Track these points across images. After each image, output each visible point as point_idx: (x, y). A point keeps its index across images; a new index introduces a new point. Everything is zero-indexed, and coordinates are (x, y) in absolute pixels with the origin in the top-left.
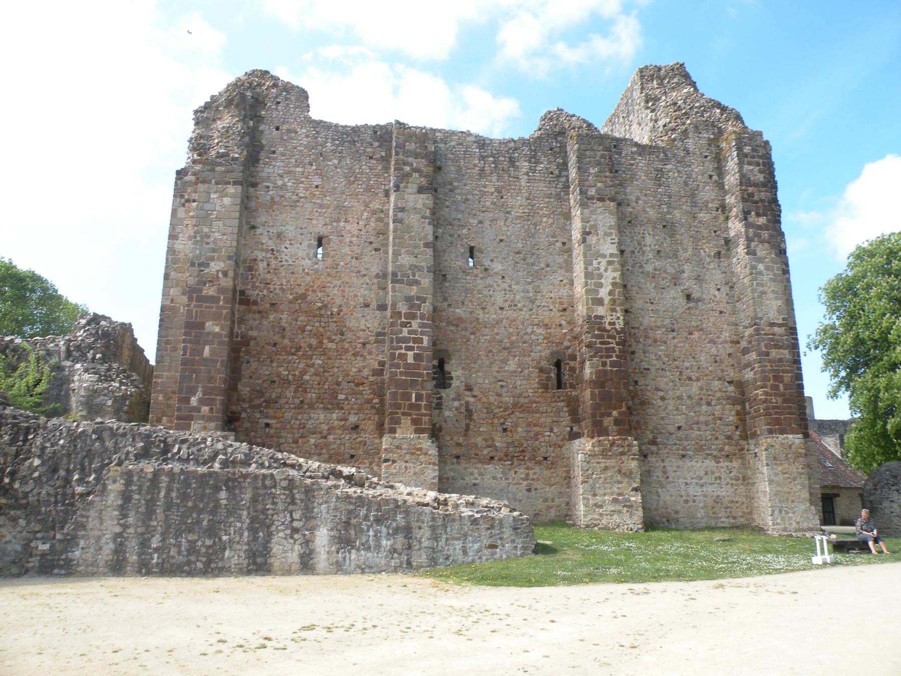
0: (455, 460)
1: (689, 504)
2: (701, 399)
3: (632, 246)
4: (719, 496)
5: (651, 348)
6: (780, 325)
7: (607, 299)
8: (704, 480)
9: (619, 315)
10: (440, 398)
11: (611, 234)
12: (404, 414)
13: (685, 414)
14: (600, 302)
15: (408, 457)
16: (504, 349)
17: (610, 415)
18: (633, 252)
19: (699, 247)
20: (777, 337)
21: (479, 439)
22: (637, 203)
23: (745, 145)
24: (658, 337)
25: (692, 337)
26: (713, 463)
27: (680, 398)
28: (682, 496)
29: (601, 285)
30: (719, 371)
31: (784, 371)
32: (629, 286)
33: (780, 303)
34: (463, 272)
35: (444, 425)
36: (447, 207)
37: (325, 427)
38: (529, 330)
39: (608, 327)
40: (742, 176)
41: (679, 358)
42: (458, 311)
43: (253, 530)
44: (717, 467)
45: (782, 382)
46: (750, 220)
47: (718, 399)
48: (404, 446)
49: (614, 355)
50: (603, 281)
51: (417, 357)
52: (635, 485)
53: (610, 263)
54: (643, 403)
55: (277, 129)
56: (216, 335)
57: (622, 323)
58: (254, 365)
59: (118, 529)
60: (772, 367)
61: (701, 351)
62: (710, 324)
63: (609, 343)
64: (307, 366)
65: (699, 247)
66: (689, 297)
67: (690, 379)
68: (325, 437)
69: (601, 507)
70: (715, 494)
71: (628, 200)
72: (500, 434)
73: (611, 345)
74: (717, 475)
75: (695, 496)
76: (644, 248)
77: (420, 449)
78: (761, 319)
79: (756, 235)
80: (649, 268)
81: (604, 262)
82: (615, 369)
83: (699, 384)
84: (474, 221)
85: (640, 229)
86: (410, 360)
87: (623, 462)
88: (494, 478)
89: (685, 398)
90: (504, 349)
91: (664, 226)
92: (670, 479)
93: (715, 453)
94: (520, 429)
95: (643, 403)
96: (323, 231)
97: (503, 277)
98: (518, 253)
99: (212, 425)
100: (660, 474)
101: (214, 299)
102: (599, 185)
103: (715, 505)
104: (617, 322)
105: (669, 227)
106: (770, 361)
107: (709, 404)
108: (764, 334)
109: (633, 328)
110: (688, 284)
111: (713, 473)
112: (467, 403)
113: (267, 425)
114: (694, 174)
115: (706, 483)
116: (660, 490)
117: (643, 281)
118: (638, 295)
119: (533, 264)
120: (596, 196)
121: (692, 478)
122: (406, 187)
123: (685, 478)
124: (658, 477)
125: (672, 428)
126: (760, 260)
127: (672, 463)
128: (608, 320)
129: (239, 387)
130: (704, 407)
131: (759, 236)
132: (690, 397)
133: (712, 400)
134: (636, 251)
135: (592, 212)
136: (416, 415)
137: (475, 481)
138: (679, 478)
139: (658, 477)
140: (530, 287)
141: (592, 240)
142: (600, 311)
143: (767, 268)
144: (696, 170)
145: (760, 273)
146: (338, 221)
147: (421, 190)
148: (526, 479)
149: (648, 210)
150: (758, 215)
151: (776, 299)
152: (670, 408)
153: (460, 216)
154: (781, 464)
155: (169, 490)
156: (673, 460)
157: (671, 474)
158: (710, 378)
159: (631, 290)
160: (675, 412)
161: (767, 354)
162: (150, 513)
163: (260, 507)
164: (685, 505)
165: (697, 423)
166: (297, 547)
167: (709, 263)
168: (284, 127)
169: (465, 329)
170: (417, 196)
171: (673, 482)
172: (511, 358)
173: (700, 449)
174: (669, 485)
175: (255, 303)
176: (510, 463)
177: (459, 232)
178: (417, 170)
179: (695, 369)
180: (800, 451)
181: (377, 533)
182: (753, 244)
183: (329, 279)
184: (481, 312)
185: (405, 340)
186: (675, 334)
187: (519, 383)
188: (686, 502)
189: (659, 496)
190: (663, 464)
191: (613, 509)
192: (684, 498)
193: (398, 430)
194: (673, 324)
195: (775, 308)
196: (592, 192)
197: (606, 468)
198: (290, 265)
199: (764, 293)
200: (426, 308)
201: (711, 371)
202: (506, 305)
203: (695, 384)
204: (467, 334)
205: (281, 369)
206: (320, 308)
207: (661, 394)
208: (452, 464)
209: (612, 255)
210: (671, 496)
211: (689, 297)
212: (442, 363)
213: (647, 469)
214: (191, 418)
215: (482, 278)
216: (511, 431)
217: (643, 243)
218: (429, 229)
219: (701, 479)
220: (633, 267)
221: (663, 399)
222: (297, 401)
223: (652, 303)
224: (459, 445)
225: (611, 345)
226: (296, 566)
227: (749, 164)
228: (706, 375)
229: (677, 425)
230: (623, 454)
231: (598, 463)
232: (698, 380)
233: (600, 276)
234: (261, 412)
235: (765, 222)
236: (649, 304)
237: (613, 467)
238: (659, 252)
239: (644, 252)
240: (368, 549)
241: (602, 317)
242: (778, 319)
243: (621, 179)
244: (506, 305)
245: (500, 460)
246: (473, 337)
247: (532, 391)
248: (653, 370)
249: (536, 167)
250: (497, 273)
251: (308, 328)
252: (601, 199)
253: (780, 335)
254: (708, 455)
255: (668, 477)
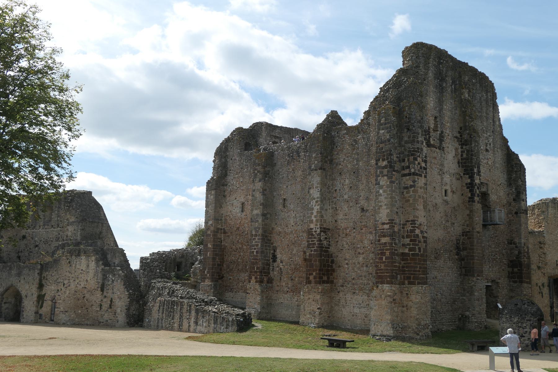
0: (276, 292)
1: (354, 317)
2: (364, 264)
3: (340, 186)
4: (366, 314)
5: (344, 238)
6: (387, 224)
7: (314, 219)
8: (362, 305)
9: (318, 227)
10: (273, 267)
11: (318, 187)
12: (253, 275)
13: (356, 271)
14: (311, 222)
15: (253, 292)
16: (293, 244)
17: (312, 274)
18: (340, 190)
19: (369, 181)
20: (385, 230)
21: (284, 284)
22: (344, 162)
23: (382, 118)
24: (347, 232)
25: (362, 231)
26: (366, 297)
27: (354, 263)
28: (351, 313)
29: (312, 213)
30: (373, 249)
31: (387, 250)
32: (337, 208)
33: (388, 211)
34: (282, 211)
35: (274, 278)
36: (277, 182)
37: (243, 279)
38: (301, 234)
39: (314, 233)
40: (378, 138)
41: (356, 243)
42: (279, 228)
43: (180, 319)
44: (368, 299)
45: (385, 255)
46: (379, 164)
47: (371, 264)
48: (252, 288)
49: (315, 246)
50: (313, 211)
51: (257, 252)
52: (319, 307)
53: (317, 202)
54: (339, 266)
55: (231, 159)
56: (210, 248)
57: (319, 231)
58: (227, 256)
59: (158, 317)
60: (380, 247)
61: (366, 238)
62: (371, 223)
63: (314, 241)
64: (239, 256)
65: (369, 181)
66: (363, 210)
67: (359, 253)
68: (243, 283)
69: (305, 315)
70: (365, 313)
71: (340, 161)
72: (290, 281)
73: (315, 242)
74: (367, 303)
75: (357, 313)
76: (345, 187)
77: (256, 289)
78: (378, 221)
79: (381, 172)
80: (346, 197)
81: (314, 201)
82: (315, 253)
83: (363, 256)
84: (285, 187)
85: (343, 176)
86: (255, 254)
87: (315, 296)
88: (288, 300)
89: (357, 263)
90: (293, 244)
91: (354, 172)
92: (348, 304)
93: (367, 292)
94: (296, 279)
95: (339, 266)
96: (243, 200)
97: (294, 211)
98: (299, 199)
99: (210, 281)
100: (344, 301)
101: (210, 235)
102: (316, 162)
103: (365, 318)
104: (317, 230)
105: (356, 172)
106: (380, 244)
107: (367, 266)
108: (379, 230)
109: (338, 229)
110: (363, 202)
111: (366, 302)
112: (281, 269)
113: (230, 278)
114: (371, 137)
115: (362, 307)
116: (343, 309)
117: (343, 204)
118: (341, 212)
119: (303, 203)
120: (315, 168)
121: (357, 304)
122: (255, 180)
123: (354, 304)
124: (343, 302)
125: (350, 279)
126: (381, 187)
127: (349, 296)
128: (314, 230)
129: (224, 265)
130: (365, 268)
131: (381, 172)
132: (359, 263)
133: (368, 264)
134: (341, 189)
135: (312, 178)
136: (256, 275)
137: (282, 301)
138: (351, 304)
139: (343, 302)
140: (302, 214)
141: (312, 191)
142: (312, 226)
143: (384, 192)
144: (372, 135)
145: (381, 195)
146: (247, 195)
147: (260, 181)
148: (297, 301)
149: (348, 165)
150: (383, 160)
151: (387, 208)
152: (350, 268)
153: (281, 185)
154: (378, 300)
155: (166, 306)
156: (349, 295)
157: (348, 302)
158: (368, 252)
159: (338, 210)
160: (352, 271)
161: (379, 241)
162: (163, 312)
163: (181, 311)
164: (352, 317)
165: (361, 276)
166: (187, 324)
167: (373, 189)
168: (233, 158)
169: (281, 236)
170: (259, 183)
171: (348, 306)
172: (294, 248)
173: (361, 289)
174: (346, 307)
175: (227, 233)
176: (292, 294)
177: (281, 193)
178: (258, 172)
179: (362, 248)
180: (388, 293)
181: (203, 321)
182: (379, 178)
183: (245, 220)
184: (286, 228)
185: (253, 246)
186: (355, 230)
187: (297, 258)
188: (353, 315)
189: (342, 312)
190: (345, 297)
191: (309, 317)
192: (352, 314)
193: (251, 282)
194: (354, 225)
195: (385, 214)
196: (313, 167)
197: (309, 298)
198: (235, 216)
199: (381, 206)
200: (260, 232)
201: (369, 249)
202: (293, 224)
203: (361, 256)
204: (282, 238)
205: (233, 258)
206: (242, 233)
207: (347, 262)
208: (276, 294)
209: (317, 198)
210: (347, 312)
211: (363, 210)
212: (275, 251)
213: (339, 299)
214: (205, 278)
215: (287, 213)
216: (294, 280)
217: (345, 184)
218: (262, 197)
219: (361, 304)
220: (340, 197)
221: (347, 264)
222: (237, 269)
223: (346, 215)
224: (278, 286)
225: (315, 242)
226: (187, 330)
227: (383, 129)
228: (367, 251)
229: (352, 277)
230: (315, 292)
231: (306, 296)
232: (363, 253)
233: (313, 209)
234: (229, 274)
235: (387, 164)
236: (345, 216)
237: (312, 298)
238: (351, 187)
239: (344, 189)
240: (201, 326)
241: (312, 229)
242: (387, 220)
243: (337, 151)
244: (293, 224)
245: (290, 292)
246: (283, 239)
247: (300, 262)
248: (344, 249)
249: (306, 154)
250: (292, 210)
251: (240, 241)
252: (316, 170)
253: (386, 230)
254: (364, 292)
255: (346, 303)
